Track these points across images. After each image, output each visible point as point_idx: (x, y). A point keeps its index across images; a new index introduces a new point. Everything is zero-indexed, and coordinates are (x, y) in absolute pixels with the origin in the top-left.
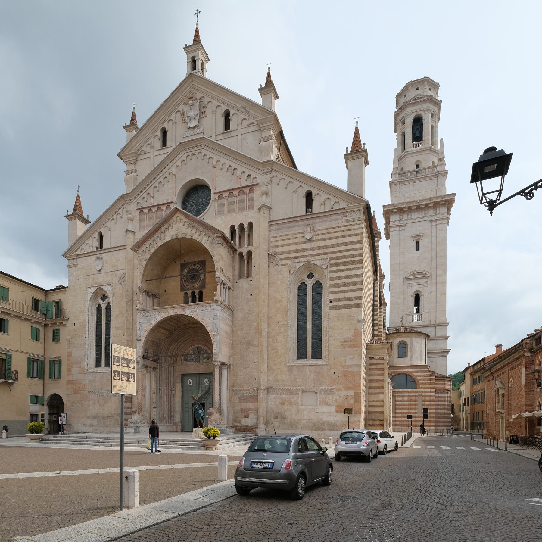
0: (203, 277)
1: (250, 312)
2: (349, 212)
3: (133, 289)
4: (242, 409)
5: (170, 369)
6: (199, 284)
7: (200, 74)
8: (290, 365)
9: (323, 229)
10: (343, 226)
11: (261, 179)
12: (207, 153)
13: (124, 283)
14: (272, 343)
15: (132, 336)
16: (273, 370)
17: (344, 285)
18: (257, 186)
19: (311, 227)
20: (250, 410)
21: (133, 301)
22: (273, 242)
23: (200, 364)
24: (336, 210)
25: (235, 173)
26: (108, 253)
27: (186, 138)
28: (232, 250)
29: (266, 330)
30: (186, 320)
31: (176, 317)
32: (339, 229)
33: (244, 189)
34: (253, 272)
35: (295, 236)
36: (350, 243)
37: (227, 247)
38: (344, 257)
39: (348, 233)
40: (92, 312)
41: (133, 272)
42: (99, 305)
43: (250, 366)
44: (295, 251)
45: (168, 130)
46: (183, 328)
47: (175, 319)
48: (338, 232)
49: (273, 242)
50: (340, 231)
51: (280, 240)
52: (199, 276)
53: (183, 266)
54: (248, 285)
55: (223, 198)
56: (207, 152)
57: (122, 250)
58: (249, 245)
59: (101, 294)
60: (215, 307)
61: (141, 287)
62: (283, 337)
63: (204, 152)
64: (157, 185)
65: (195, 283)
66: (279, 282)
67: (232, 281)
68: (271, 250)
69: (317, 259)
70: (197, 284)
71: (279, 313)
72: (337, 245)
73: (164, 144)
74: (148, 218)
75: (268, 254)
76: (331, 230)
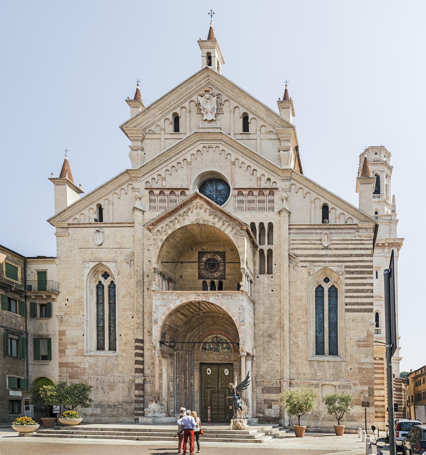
0: (223, 268)
2: (361, 228)
6: (219, 274)
7: (216, 71)
9: (338, 240)
10: (356, 240)
11: (281, 184)
12: (225, 148)
13: (132, 263)
15: (143, 319)
17: (358, 291)
18: (277, 190)
21: (143, 282)
22: (293, 244)
23: (220, 353)
24: (349, 225)
25: (254, 174)
26: (111, 228)
27: (202, 129)
28: (253, 246)
29: (288, 325)
30: (206, 308)
31: (197, 303)
32: (353, 242)
33: (264, 191)
34: (274, 270)
35: (313, 242)
36: (362, 255)
37: (250, 241)
38: (357, 267)
39: (360, 246)
44: (314, 256)
46: (202, 316)
47: (195, 306)
48: (351, 244)
49: (293, 244)
50: (354, 244)
51: (300, 244)
53: (201, 254)
54: (269, 281)
55: (242, 195)
56: (226, 148)
57: (128, 228)
58: (268, 244)
60: (241, 297)
61: (156, 268)
63: (222, 147)
64: (169, 168)
66: (299, 282)
67: (253, 275)
68: (291, 251)
69: (333, 265)
72: (351, 255)
73: (177, 129)
76: (346, 242)
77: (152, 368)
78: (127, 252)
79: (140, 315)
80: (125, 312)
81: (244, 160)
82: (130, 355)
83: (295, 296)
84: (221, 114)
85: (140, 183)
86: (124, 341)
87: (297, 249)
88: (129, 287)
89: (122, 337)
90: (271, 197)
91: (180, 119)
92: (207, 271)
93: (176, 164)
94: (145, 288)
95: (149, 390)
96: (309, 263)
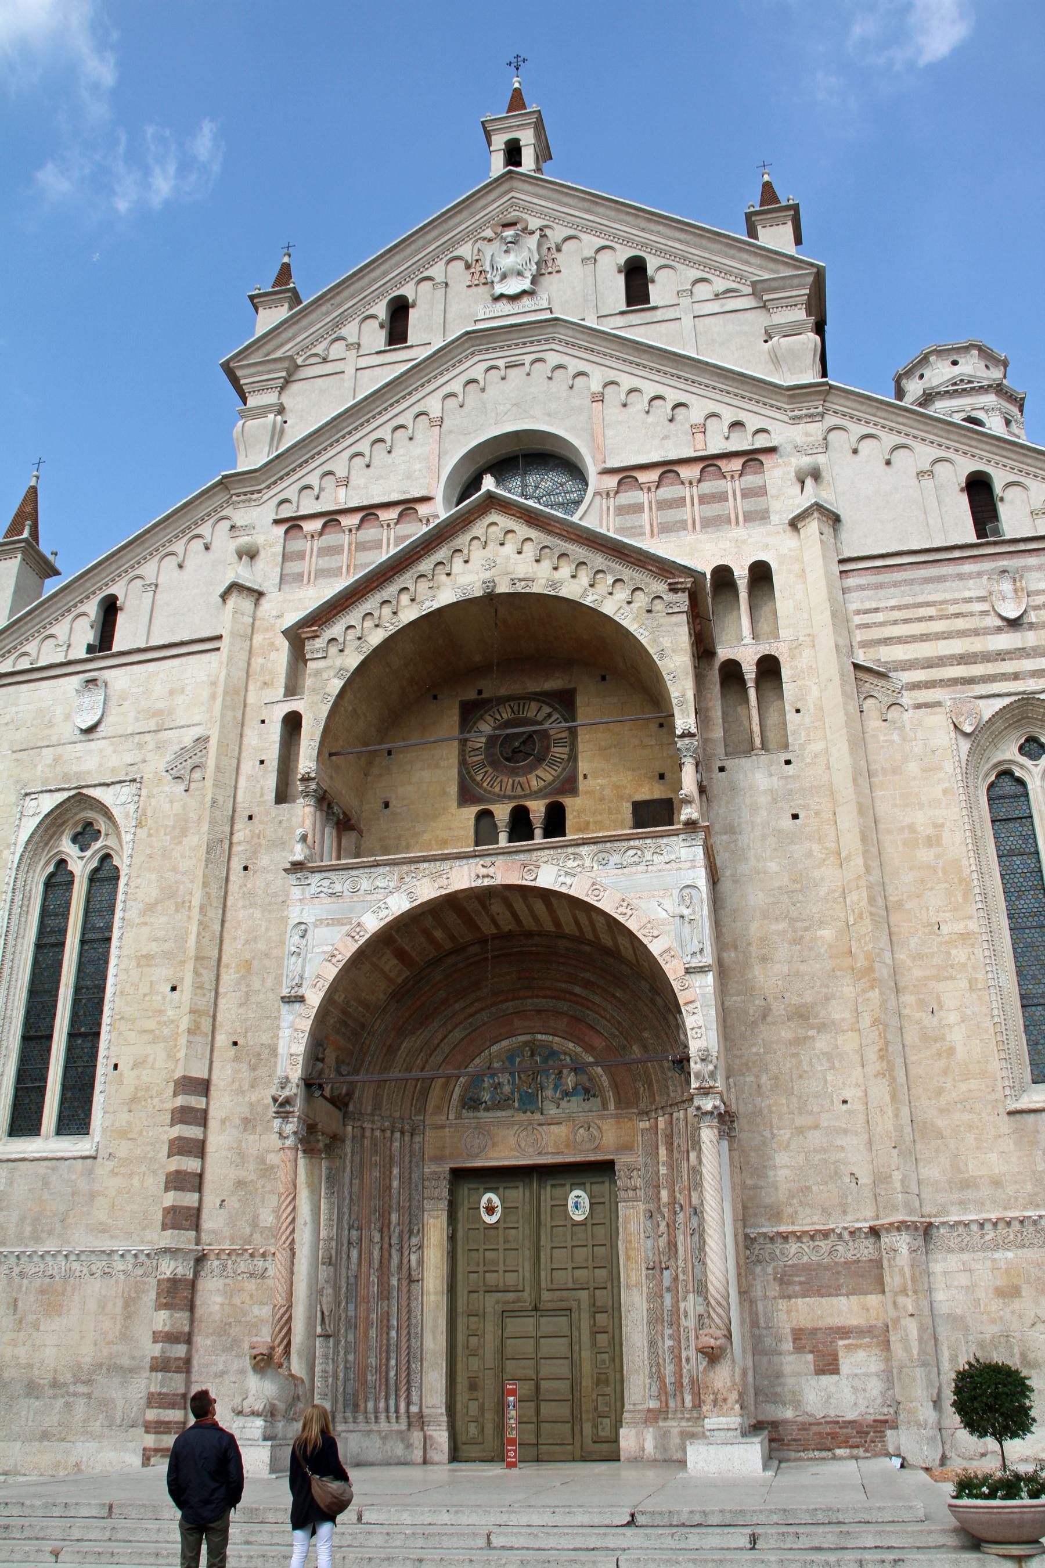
0: (566, 750)
1: (798, 886)
3: (235, 797)
4: (798, 1334)
5: (397, 1144)
6: (549, 778)
8: (1024, 1103)
13: (197, 775)
14: (918, 1015)
16: (941, 1136)
19: (1015, 581)
20: (844, 1332)
21: (231, 844)
26: (135, 667)
33: (722, 464)
35: (952, 609)
40: (27, 894)
41: (241, 736)
42: (62, 863)
43: (824, 1124)
44: (963, 659)
45: (414, 301)
49: (866, 626)
51: (895, 622)
52: (548, 748)
53: (470, 712)
59: (76, 824)
62: (964, 984)
63: (553, 359)
65: (530, 773)
66: (913, 768)
70: (540, 777)
71: (932, 889)
74: (319, 549)
75: (856, 666)
77: (237, 1205)
78: (180, 742)
79: (208, 977)
80: (146, 970)
81: (637, 383)
82: (149, 1148)
83: (902, 829)
84: (550, 273)
85: (259, 509)
86: (127, 1091)
87: (887, 641)
88: (174, 869)
89: (121, 1075)
90: (751, 480)
91: (411, 310)
92: (495, 769)
93: (389, 431)
94: (236, 865)
95: (217, 1307)
96: (947, 689)
